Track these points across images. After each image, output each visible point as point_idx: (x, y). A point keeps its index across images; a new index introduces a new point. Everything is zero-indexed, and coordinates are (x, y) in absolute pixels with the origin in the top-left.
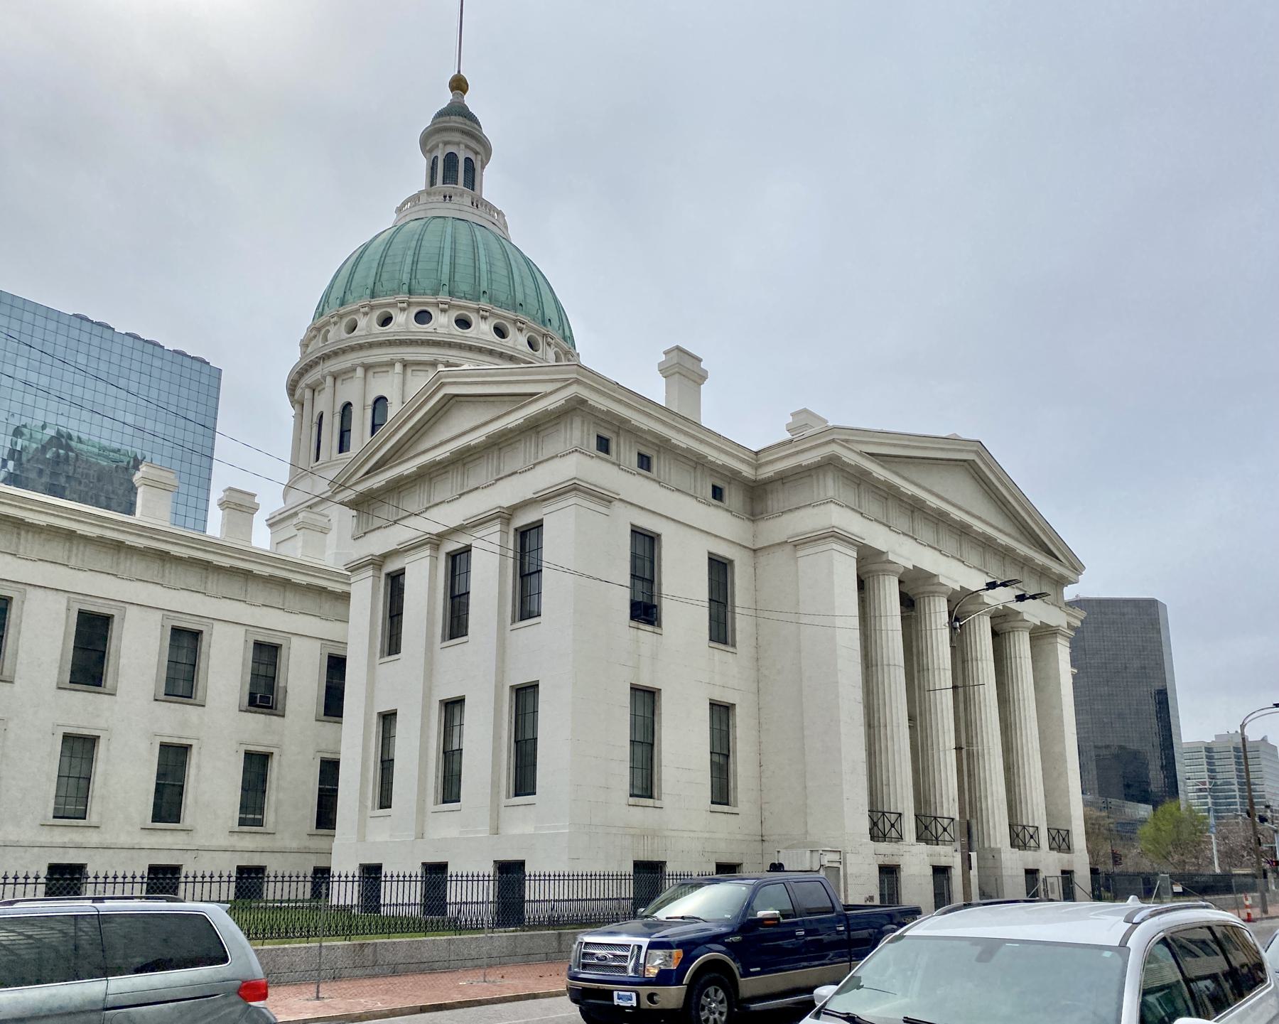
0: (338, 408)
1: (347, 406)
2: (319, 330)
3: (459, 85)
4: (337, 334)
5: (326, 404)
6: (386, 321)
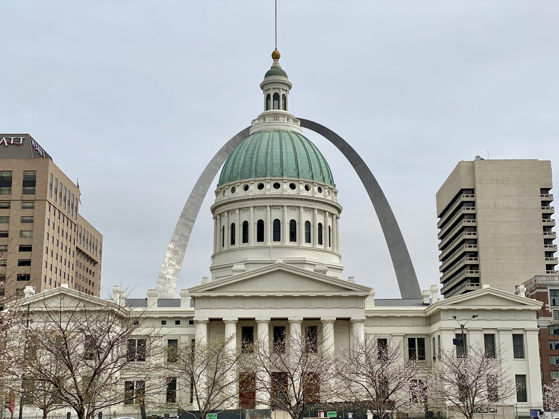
0: (230, 226)
1: (233, 225)
2: (221, 189)
3: (276, 56)
4: (228, 195)
5: (226, 222)
6: (246, 188)
